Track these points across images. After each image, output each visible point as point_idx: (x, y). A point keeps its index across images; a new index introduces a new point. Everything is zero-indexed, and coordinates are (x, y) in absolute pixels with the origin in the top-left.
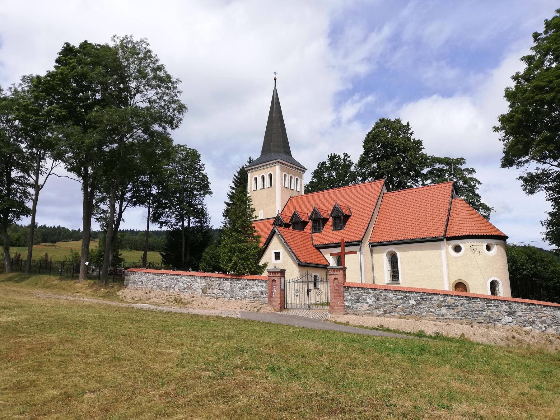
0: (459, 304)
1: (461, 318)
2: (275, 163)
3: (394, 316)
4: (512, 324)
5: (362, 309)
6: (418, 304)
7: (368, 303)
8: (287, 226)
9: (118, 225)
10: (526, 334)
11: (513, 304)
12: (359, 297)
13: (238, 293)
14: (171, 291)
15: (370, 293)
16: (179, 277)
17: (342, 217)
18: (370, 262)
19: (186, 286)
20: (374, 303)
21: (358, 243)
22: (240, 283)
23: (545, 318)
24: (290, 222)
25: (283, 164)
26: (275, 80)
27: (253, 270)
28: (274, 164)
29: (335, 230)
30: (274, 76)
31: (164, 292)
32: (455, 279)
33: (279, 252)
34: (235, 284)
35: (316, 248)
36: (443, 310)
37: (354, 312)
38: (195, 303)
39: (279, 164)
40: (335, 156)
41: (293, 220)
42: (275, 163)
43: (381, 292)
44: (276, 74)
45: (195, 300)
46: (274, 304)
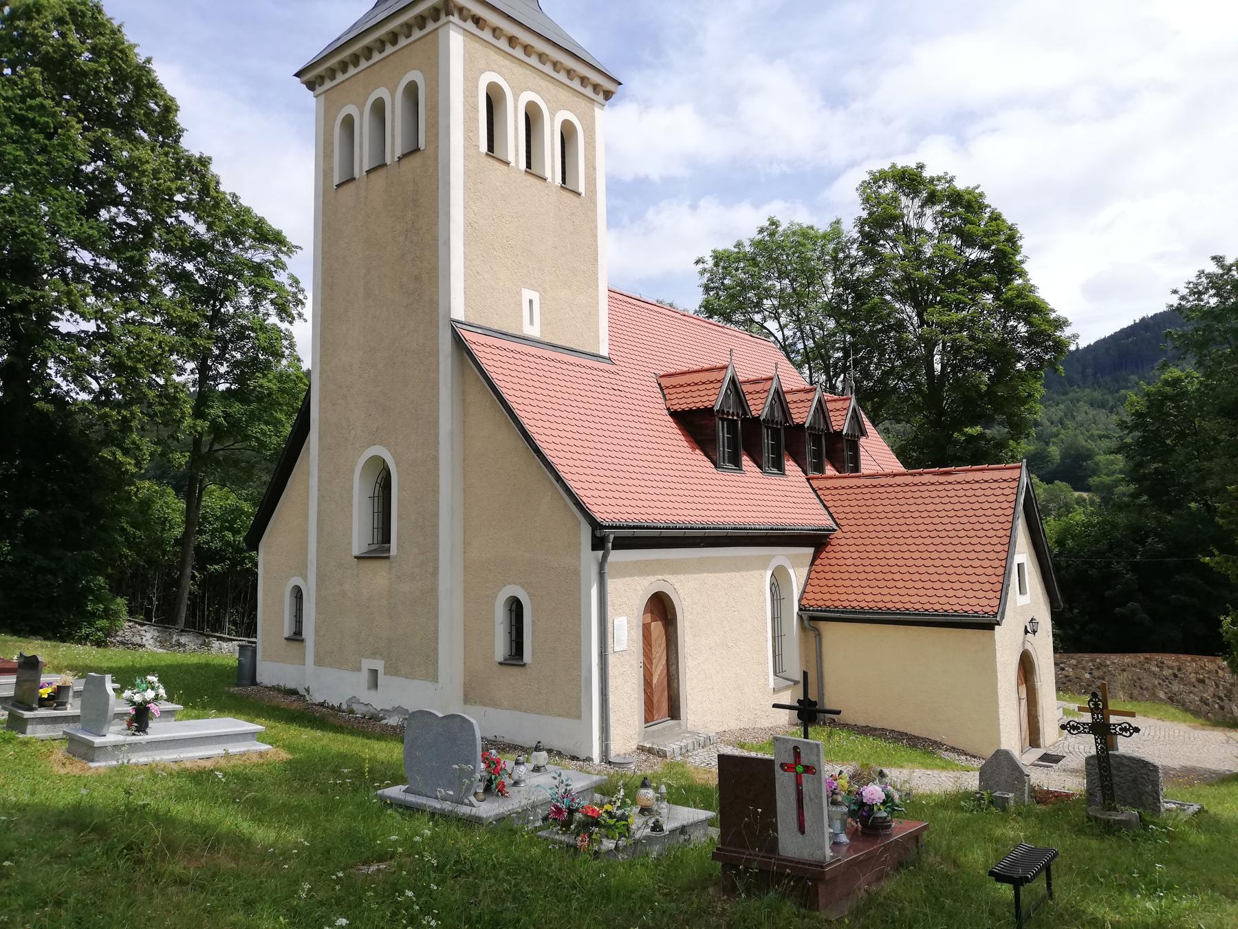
28: (431, 26)
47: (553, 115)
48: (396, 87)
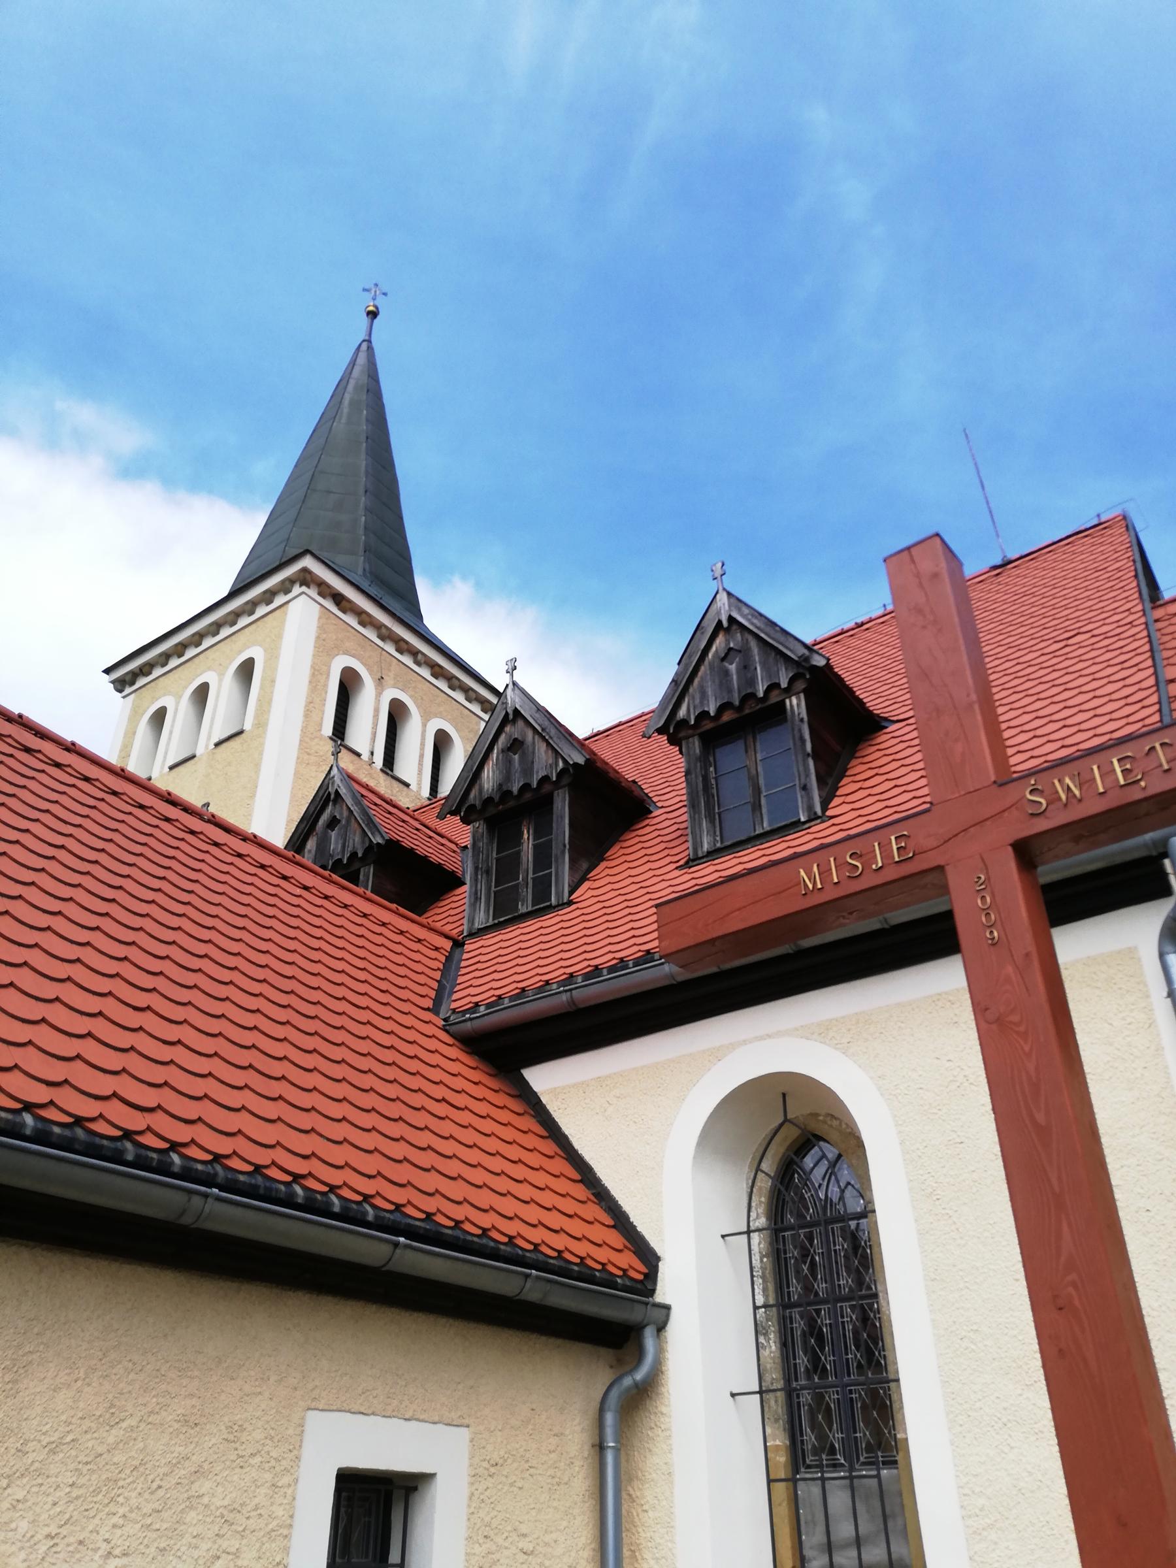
25: (339, 599)
28: (279, 600)
39: (313, 592)
48: (227, 668)
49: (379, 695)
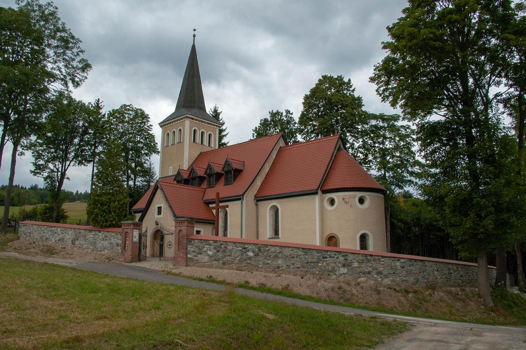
0: (295, 256)
1: (296, 269)
2: (185, 117)
3: (232, 268)
4: (347, 275)
5: (203, 261)
6: (255, 256)
7: (208, 255)
8: (187, 182)
9: (61, 183)
10: (355, 285)
11: (350, 255)
12: (201, 249)
13: (99, 244)
14: (50, 242)
15: (211, 245)
16: (55, 228)
17: (232, 172)
18: (254, 217)
19: (60, 237)
20: (214, 254)
21: (238, 198)
22: (101, 235)
23: (382, 269)
24: (188, 177)
25: (192, 119)
26: (194, 36)
27: (114, 222)
28: (184, 120)
29: (226, 185)
30: (193, 33)
31: (44, 243)
32: (327, 233)
33: (161, 207)
34: (97, 236)
35: (205, 203)
36: (280, 262)
37: (195, 264)
38: (62, 253)
39: (188, 119)
40: (278, 113)
41: (191, 176)
42: (185, 118)
43: (222, 244)
44: (196, 31)
45: (64, 251)
46: (126, 256)
47: (207, 133)
49: (199, 131)
